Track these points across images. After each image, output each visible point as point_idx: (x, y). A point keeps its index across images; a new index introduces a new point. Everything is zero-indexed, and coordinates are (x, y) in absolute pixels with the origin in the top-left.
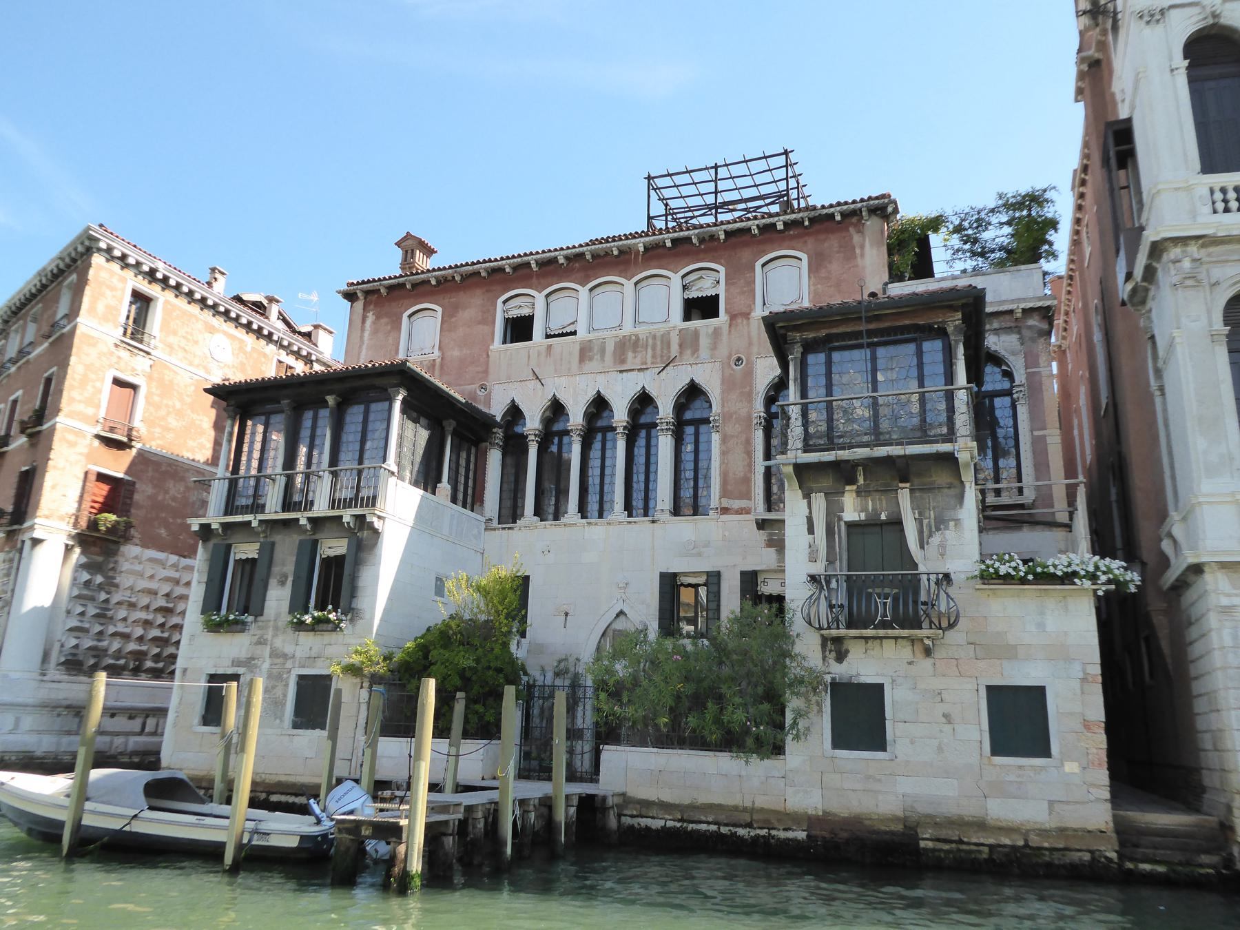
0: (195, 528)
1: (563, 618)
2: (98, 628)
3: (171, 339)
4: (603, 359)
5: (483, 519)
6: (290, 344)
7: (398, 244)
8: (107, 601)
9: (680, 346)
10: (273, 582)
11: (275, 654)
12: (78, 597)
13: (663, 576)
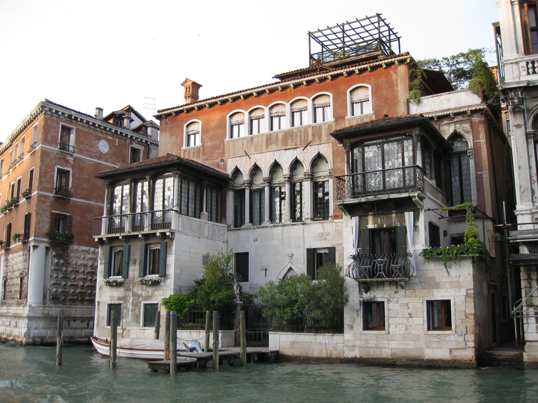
0: (96, 240)
1: (264, 272)
2: (64, 283)
3: (81, 146)
4: (277, 144)
5: (226, 226)
6: (136, 138)
7: (182, 85)
8: (66, 271)
9: (313, 135)
10: (131, 263)
11: (134, 295)
12: (54, 270)
13: (308, 250)
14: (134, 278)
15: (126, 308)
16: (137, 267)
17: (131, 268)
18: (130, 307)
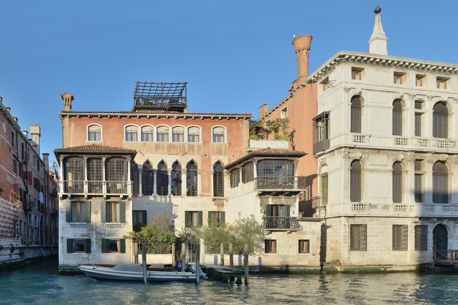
9: (188, 149)
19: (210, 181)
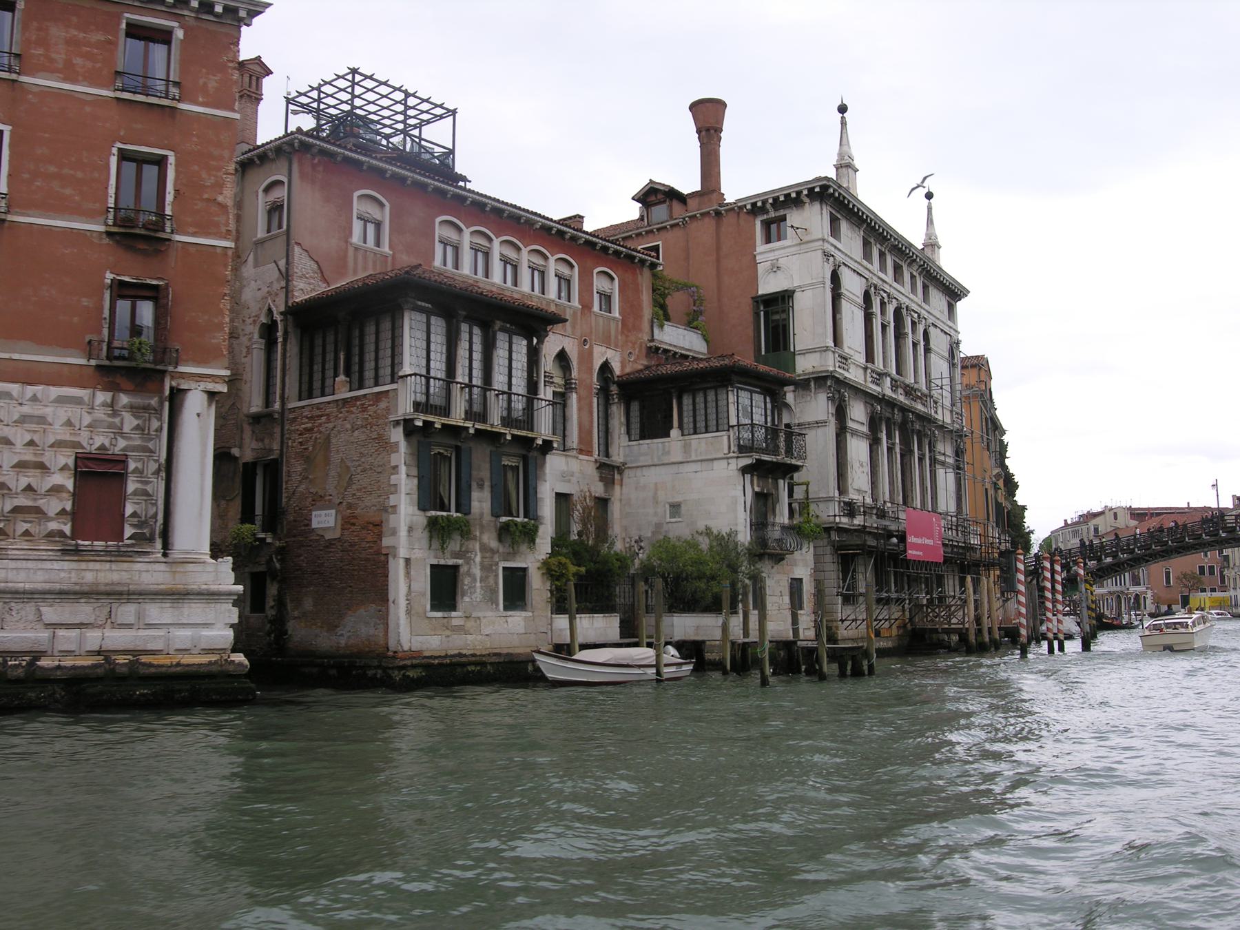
10: (474, 485)
14: (482, 515)
15: (469, 574)
16: (487, 494)
17: (475, 495)
18: (477, 571)
19: (591, 413)
